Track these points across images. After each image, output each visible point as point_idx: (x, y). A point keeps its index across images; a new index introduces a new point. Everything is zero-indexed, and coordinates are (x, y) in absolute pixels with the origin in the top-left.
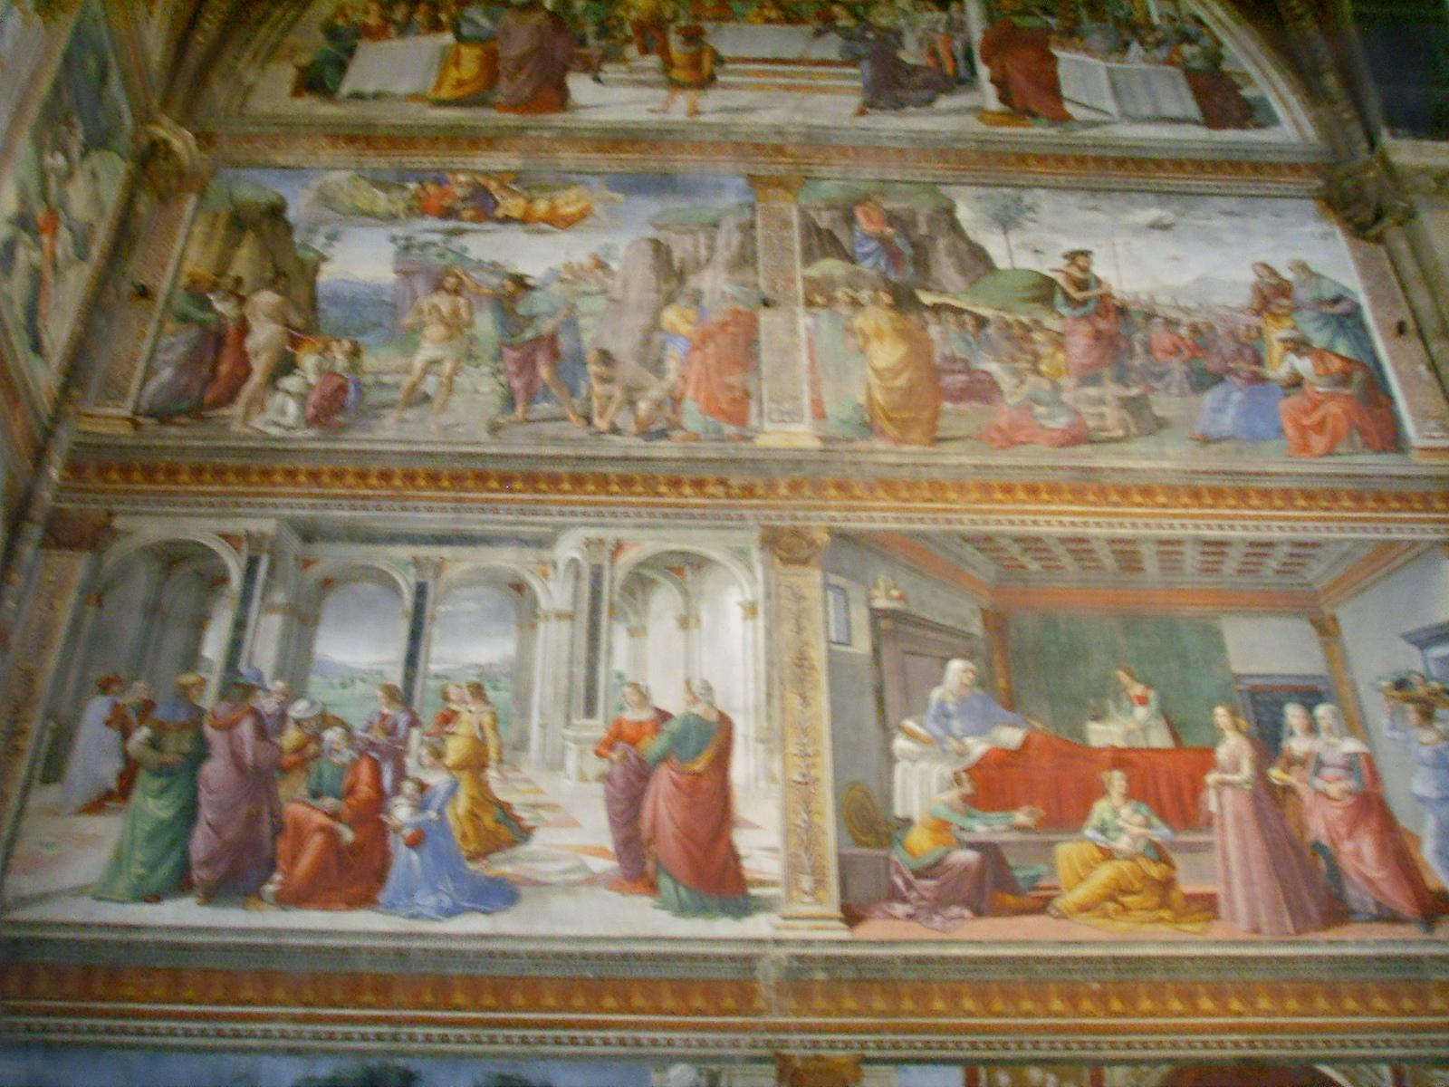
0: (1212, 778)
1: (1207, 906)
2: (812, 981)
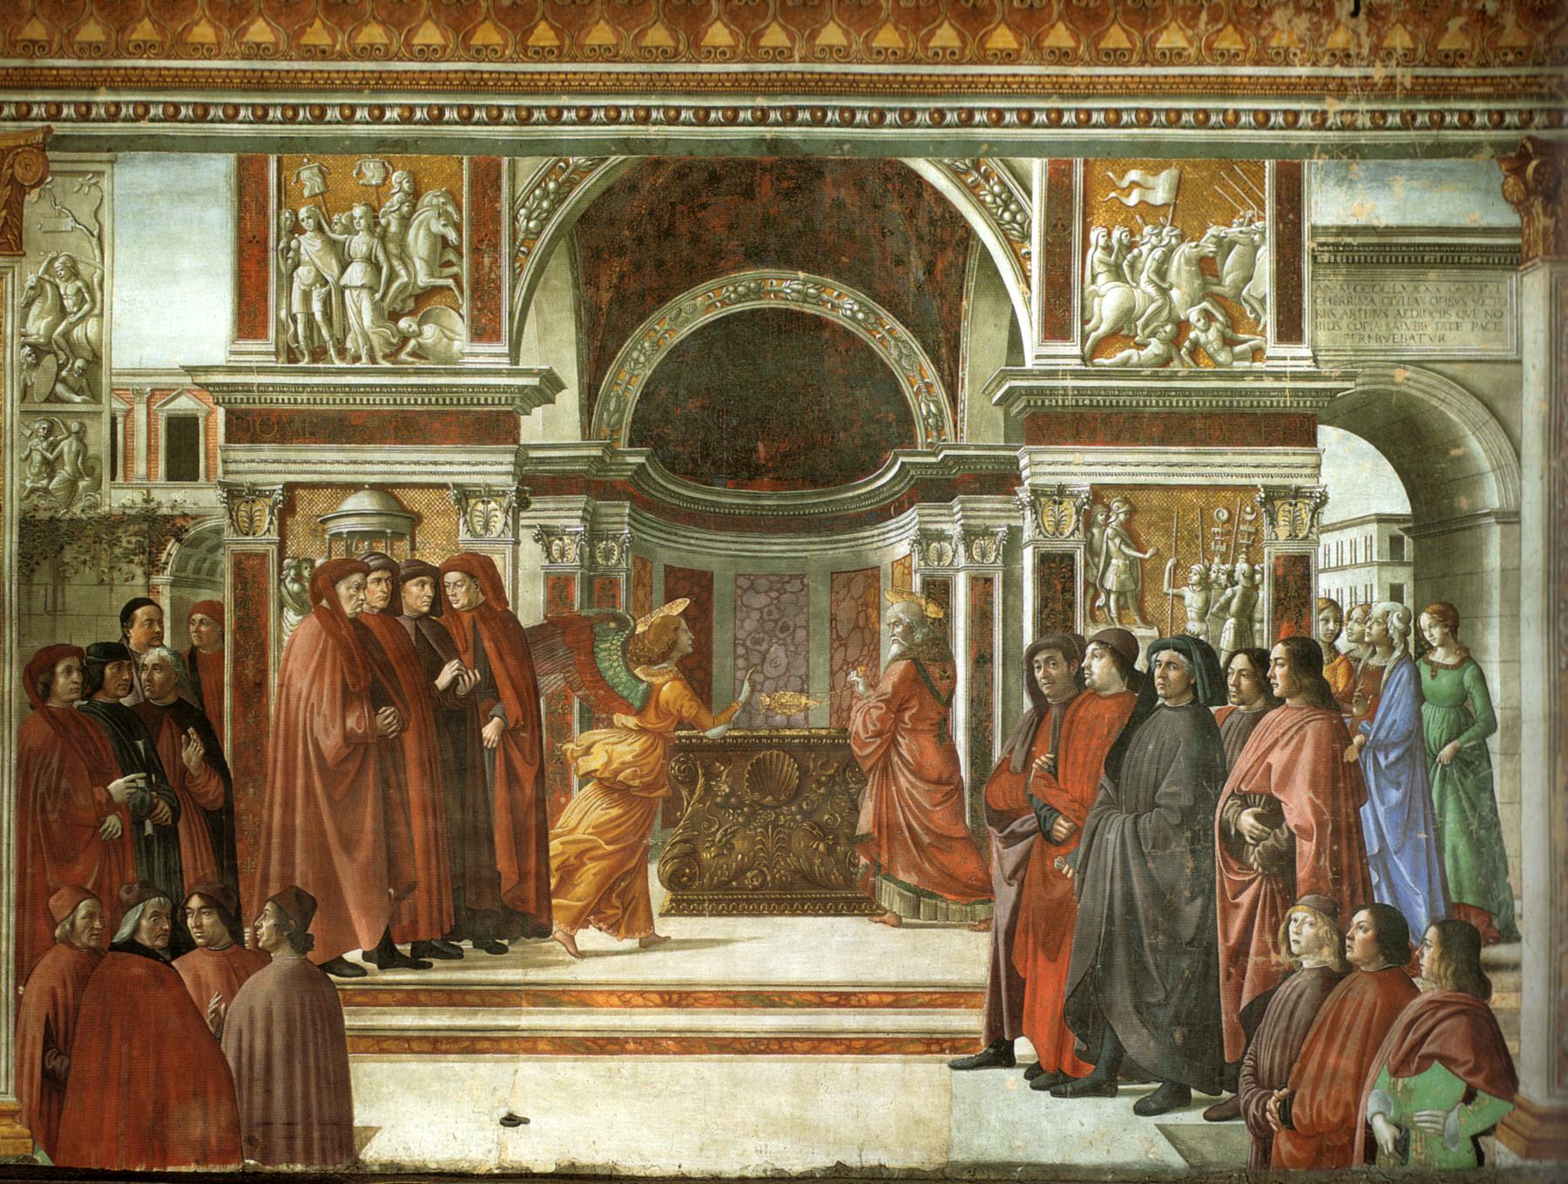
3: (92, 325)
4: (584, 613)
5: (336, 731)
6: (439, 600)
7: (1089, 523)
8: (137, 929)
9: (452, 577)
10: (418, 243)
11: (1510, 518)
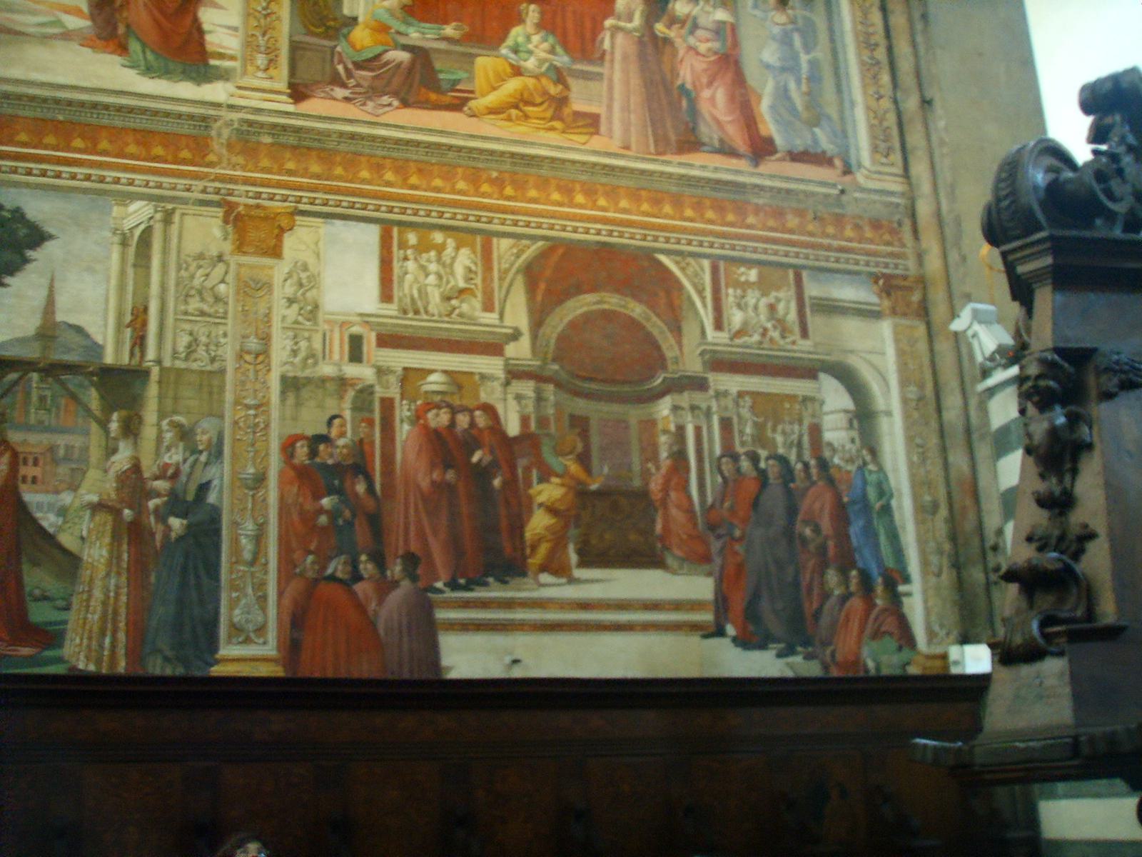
0: (609, 22)
1: (591, 123)
2: (259, 143)
3: (314, 292)
4: (537, 432)
5: (428, 480)
6: (473, 424)
7: (737, 405)
8: (336, 569)
9: (478, 413)
10: (459, 270)
11: (889, 413)
